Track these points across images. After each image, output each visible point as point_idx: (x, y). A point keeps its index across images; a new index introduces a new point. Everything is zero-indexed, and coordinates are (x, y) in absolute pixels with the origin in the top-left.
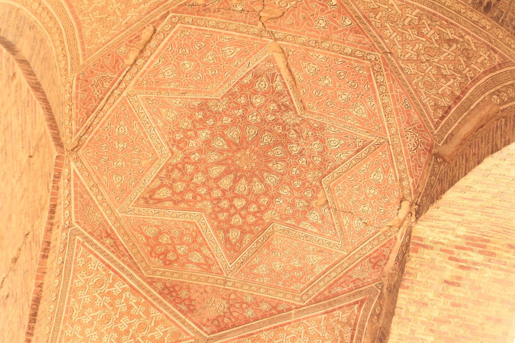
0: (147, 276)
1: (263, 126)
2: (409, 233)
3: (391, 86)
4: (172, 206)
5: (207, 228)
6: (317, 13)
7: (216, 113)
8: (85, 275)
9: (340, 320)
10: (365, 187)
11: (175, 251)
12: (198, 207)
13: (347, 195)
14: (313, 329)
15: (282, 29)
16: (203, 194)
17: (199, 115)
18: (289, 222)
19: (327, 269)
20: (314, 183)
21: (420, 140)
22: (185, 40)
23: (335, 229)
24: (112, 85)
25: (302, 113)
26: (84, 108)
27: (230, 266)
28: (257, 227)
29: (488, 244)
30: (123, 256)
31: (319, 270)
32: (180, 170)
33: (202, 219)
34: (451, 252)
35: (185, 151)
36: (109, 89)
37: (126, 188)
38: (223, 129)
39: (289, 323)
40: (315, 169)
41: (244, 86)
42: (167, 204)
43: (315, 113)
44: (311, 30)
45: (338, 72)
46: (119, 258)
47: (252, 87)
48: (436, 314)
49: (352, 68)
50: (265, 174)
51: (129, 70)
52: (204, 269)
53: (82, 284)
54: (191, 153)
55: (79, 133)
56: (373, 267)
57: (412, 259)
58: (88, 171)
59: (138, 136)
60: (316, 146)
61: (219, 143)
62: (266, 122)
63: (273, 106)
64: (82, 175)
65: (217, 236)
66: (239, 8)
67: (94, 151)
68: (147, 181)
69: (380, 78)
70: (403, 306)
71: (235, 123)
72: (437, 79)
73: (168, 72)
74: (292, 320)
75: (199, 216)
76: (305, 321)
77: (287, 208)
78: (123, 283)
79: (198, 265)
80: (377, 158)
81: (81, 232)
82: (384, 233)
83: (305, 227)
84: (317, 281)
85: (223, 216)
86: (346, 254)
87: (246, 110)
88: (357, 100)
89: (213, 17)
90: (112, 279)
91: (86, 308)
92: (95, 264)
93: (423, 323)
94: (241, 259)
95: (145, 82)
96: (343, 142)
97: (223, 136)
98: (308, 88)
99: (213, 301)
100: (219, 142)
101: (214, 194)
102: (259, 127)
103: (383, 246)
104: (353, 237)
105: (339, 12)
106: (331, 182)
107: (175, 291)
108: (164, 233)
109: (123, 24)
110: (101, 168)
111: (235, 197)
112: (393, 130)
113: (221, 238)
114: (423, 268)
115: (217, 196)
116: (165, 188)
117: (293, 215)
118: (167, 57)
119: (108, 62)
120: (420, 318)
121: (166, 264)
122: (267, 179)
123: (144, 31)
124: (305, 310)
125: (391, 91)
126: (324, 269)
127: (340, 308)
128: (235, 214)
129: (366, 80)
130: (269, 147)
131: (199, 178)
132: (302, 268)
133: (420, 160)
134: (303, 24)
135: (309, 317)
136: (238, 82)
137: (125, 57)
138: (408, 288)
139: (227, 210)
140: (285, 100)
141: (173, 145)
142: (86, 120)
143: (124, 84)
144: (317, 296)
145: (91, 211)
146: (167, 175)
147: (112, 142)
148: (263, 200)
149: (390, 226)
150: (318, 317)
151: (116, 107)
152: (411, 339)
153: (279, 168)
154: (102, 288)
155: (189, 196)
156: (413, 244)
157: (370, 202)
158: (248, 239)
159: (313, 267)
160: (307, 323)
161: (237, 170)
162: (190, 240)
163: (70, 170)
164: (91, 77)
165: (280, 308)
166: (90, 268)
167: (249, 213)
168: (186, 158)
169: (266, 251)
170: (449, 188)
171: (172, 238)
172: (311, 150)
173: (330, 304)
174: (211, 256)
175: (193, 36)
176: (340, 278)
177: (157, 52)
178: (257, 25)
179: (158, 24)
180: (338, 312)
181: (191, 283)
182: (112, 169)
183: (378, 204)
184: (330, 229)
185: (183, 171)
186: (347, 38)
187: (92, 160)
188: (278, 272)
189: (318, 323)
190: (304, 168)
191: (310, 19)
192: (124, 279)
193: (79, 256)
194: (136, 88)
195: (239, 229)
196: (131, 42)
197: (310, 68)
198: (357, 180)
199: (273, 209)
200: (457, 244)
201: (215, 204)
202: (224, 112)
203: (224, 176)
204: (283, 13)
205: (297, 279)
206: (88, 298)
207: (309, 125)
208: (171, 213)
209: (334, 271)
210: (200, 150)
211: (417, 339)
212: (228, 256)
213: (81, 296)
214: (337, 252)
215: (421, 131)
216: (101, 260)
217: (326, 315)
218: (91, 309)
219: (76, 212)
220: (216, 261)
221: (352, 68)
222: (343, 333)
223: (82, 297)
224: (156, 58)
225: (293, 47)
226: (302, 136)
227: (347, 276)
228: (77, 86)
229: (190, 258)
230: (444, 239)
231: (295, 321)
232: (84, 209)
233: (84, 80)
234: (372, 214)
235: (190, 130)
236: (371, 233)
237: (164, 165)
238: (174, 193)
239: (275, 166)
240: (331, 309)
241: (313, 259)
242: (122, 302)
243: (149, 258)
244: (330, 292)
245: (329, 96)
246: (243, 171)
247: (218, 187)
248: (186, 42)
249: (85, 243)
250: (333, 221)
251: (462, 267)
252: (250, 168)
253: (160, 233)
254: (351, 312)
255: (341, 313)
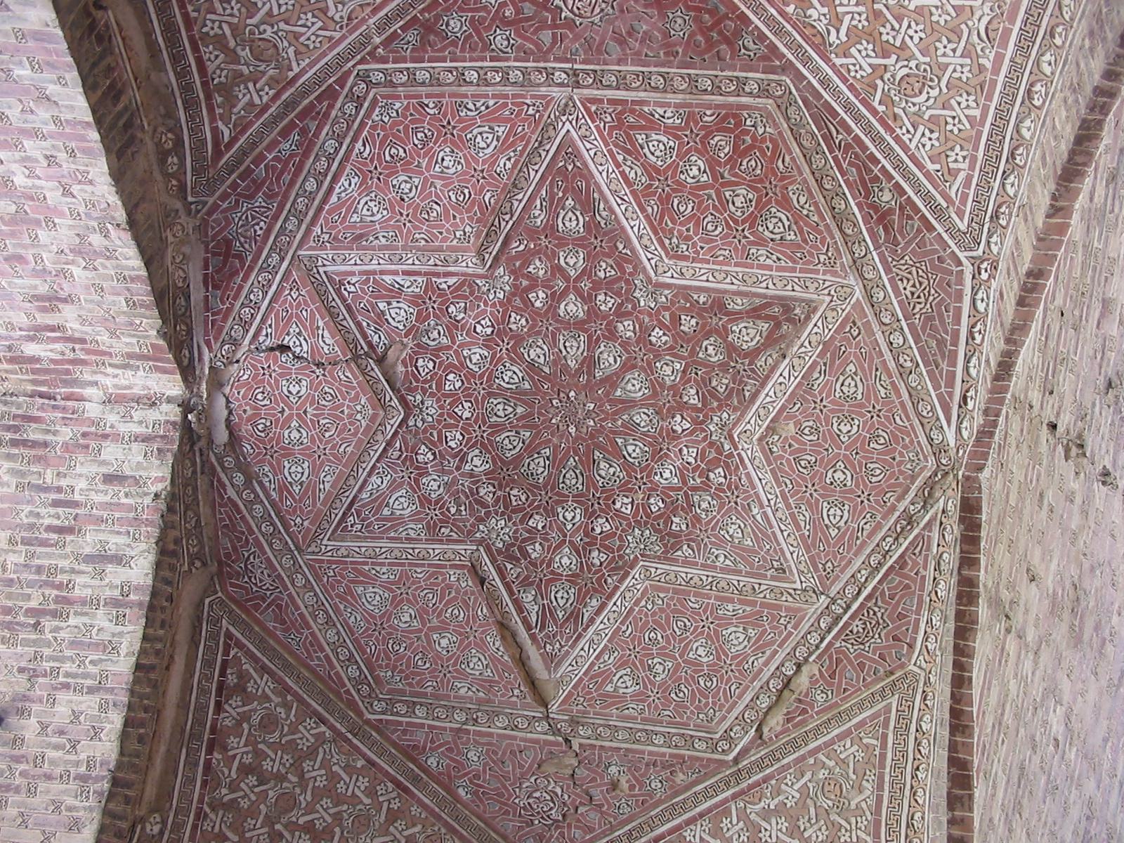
0: (784, 78)
1: (550, 496)
2: (188, 372)
3: (332, 666)
4: (727, 296)
5: (640, 238)
6: (484, 771)
7: (646, 523)
8: (950, 120)
9: (251, 85)
10: (313, 441)
11: (713, 164)
12: (666, 292)
13: (343, 405)
14: (310, 29)
15: (536, 741)
16: (657, 330)
17: (678, 523)
18: (452, 281)
19: (330, 190)
20: (419, 397)
21: (246, 579)
22: (707, 704)
23: (344, 300)
24: (847, 624)
25: (476, 554)
26: (906, 577)
27: (568, 125)
28: (522, 247)
29: (31, 377)
30: (848, 146)
31: (347, 185)
32: (713, 393)
33: (653, 262)
34: (88, 352)
35: (705, 439)
36: (852, 617)
37: (833, 362)
38: (628, 482)
39: (375, 10)
40: (425, 431)
41: (595, 590)
42: (738, 304)
43: (452, 566)
44: (489, 744)
45: (428, 665)
46: (857, 139)
47: (580, 589)
48: (43, 235)
49: (407, 678)
50: (527, 386)
51: (810, 654)
52: (632, 111)
53: (959, 99)
54: (691, 433)
55: (927, 518)
56: (228, 243)
57: (155, 333)
58: (919, 414)
59: (802, 498)
60: (433, 484)
61: (634, 450)
62: (545, 509)
63: (535, 551)
64: (933, 409)
65: (612, 211)
66: (613, 770)
67: (900, 463)
68: (786, 374)
69: (353, 671)
70: (118, 243)
71: (607, 499)
72: (258, 754)
73: (737, 639)
74: (371, 21)
75: (660, 270)
76: (337, 35)
77: (462, 315)
78: (849, 71)
79: (651, 124)
80: (311, 511)
81: (952, 237)
82: (236, 343)
83: (412, 278)
84: (344, 147)
85: (605, 270)
86: (300, 252)
87: (586, 534)
88: (382, 617)
89: (657, 754)
90: (875, 88)
91: (950, 26)
92: (922, 142)
93: (61, 215)
94: (543, 154)
95: (782, 621)
96: (386, 512)
97: (627, 466)
98: (474, 622)
99: (597, 10)
100: (634, 455)
101: (631, 328)
102: (558, 494)
103: (229, 310)
104: (299, 304)
105: (449, 777)
106: (385, 417)
107: (705, 31)
108: (744, 222)
109: (808, 775)
110: (886, 417)
111: (583, 322)
112: (300, 581)
113: (602, 206)
114: (121, 319)
115: (626, 323)
116: (745, 347)
117: (445, 304)
118: (739, 671)
119: (851, 673)
120: (71, 222)
121: (735, 116)
122: (520, 375)
123: (779, 728)
124: (348, 60)
125: (327, 657)
126: (337, 190)
127: (265, 108)
128: (578, 279)
129: (377, 660)
130: (531, 449)
131: (668, 370)
132: (388, 176)
133: (231, 541)
134: (504, 754)
135: (331, 49)
136: (610, 597)
137: (817, 681)
138: (133, 279)
139: (597, 285)
140: (512, 571)
141: (730, 456)
142: (907, 549)
143: (823, 625)
144: (331, 106)
145: (922, 300)
146: (741, 382)
147: (857, 486)
148: (518, 322)
149: (231, 363)
150: (307, 61)
151: (842, 571)
152: (63, 176)
153: (500, 407)
154: (905, 71)
155: (688, 324)
156: (168, 361)
157: (291, 408)
158: (537, 213)
159: (364, 188)
160: (328, 34)
161: (589, 388)
162: (676, 202)
163: (959, 430)
164: (885, 647)
165: (411, 36)
166: (935, 135)
167: (546, 285)
168: (702, 422)
169: (487, 199)
170: (154, 594)
171: (724, 203)
172: (443, 472)
173: (289, 105)
174: (620, 158)
175: (692, 712)
176: (292, 183)
177: (757, 684)
178: (581, 745)
179: (752, 742)
180: (265, 99)
181: (663, 65)
182: (863, 415)
183: (274, 409)
184: (357, 297)
185: (707, 394)
186: (427, 736)
187: (907, 440)
188: (445, 142)
189: (303, 49)
190: (446, 426)
191: (494, 762)
192: (844, 80)
193: (962, 176)
194: (799, 610)
195: (564, 238)
196: (804, 711)
197: (477, 665)
198: (333, 448)
199: (494, 305)
200: (86, 369)
201: (627, 299)
202: (629, 525)
203: (616, 374)
204: (539, 766)
205: (394, 136)
206: (944, 55)
207: (458, 528)
208: (728, 280)
209: (311, 197)
210: (674, 439)
211: (49, 178)
212: (577, 155)
213: (962, 66)
214: (323, 248)
215: (250, 600)
216: (905, 148)
217: (291, 74)
218: (935, 18)
219: (959, 296)
220: (607, 145)
221: (407, 678)
222: (228, 59)
223: (961, 61)
224: (761, 670)
225: (513, 706)
226: (467, 497)
227: (277, 194)
228: (916, 631)
229: (671, 143)
230: (116, 376)
231: (364, 20)
232: (939, 304)
233: (900, 640)
234: (276, 381)
235: (694, 489)
236: (264, 333)
237: (748, 407)
238: (724, 333)
239: (510, 410)
240: (284, 97)
241: (370, 210)
242: (848, 17)
243: (780, 133)
244: (304, 132)
245: (434, 612)
246: (576, 386)
247: (625, 344)
248: (704, 701)
249: (945, 205)
250: (354, 318)
251: (53, 329)
252: (562, 395)
253: (752, 220)
254: (234, 117)
255: (257, 101)
